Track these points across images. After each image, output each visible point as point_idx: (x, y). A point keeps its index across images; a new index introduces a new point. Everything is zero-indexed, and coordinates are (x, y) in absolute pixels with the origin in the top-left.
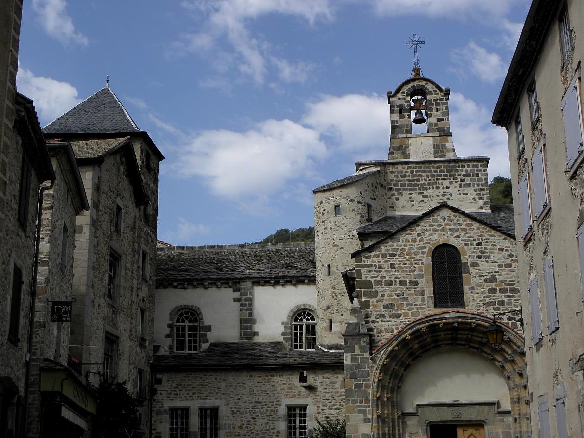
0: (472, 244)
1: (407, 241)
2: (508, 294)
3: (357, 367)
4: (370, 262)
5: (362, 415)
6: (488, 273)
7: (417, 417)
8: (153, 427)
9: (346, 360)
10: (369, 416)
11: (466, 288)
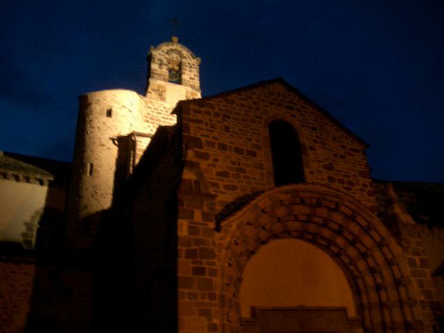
0: (308, 127)
1: (243, 105)
2: (346, 185)
4: (200, 117)
5: (204, 318)
6: (326, 159)
9: (181, 230)
10: (216, 321)
11: (306, 171)
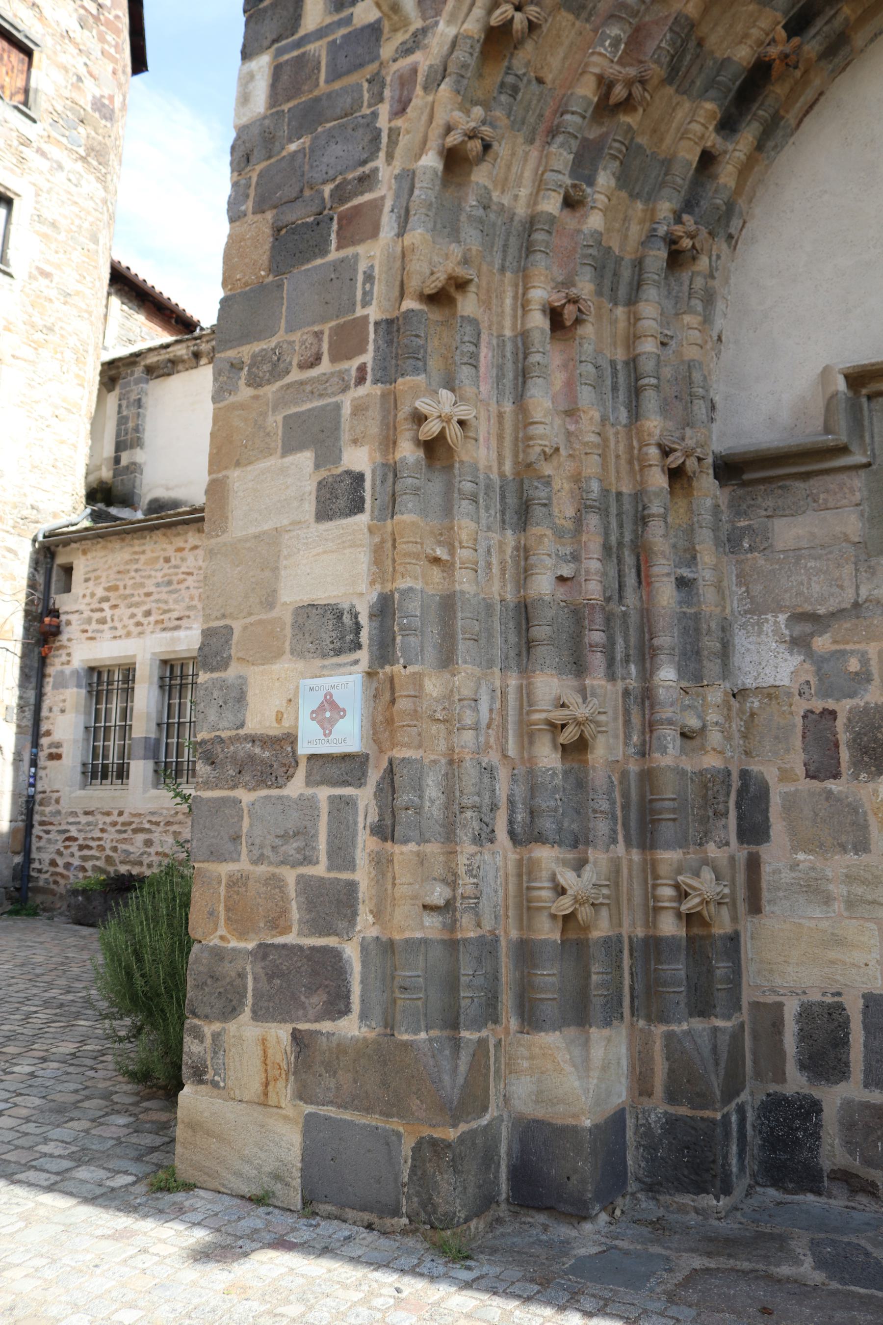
3: (309, 118)
5: (305, 459)
7: (858, 482)
8: (44, 728)
10: (359, 458)
